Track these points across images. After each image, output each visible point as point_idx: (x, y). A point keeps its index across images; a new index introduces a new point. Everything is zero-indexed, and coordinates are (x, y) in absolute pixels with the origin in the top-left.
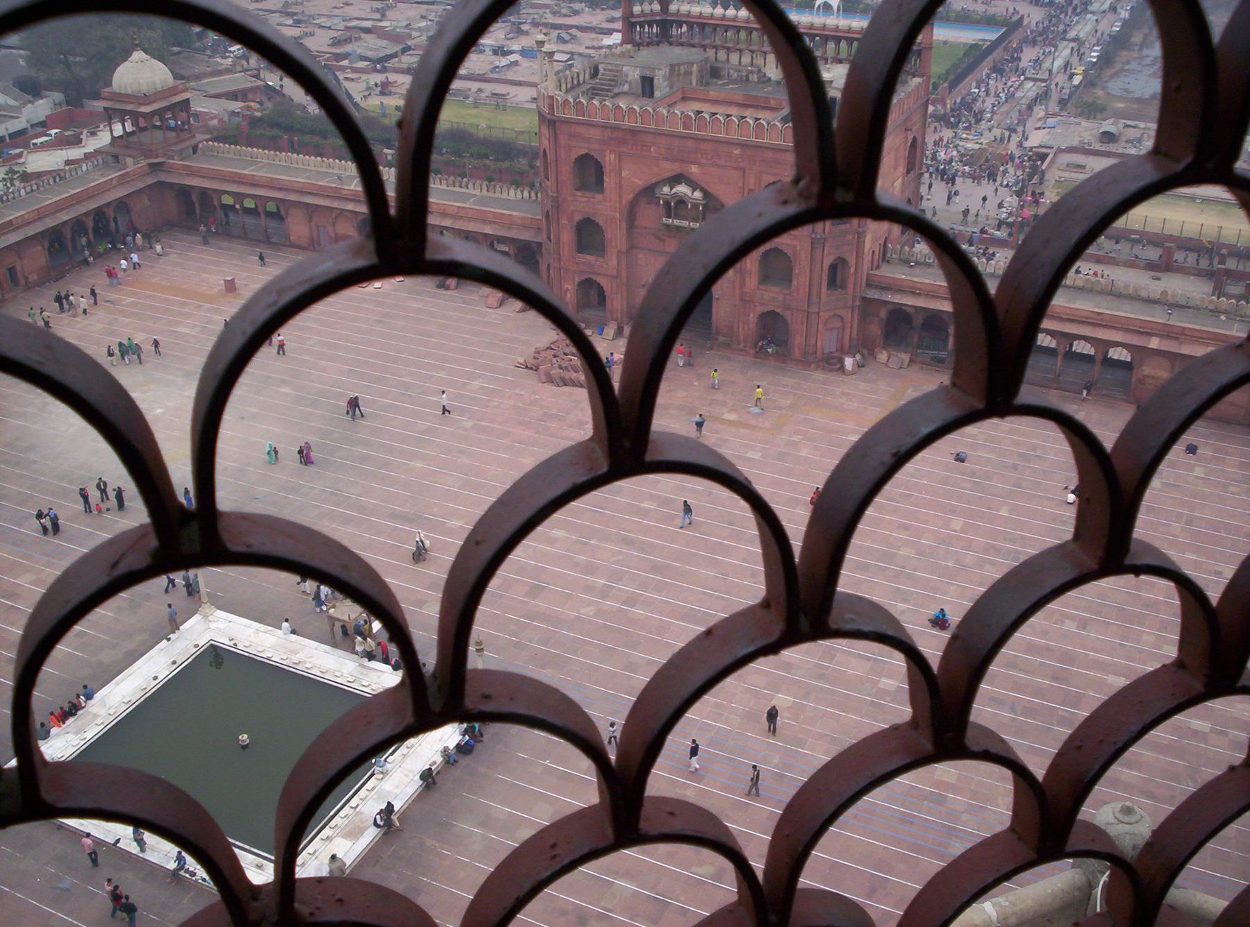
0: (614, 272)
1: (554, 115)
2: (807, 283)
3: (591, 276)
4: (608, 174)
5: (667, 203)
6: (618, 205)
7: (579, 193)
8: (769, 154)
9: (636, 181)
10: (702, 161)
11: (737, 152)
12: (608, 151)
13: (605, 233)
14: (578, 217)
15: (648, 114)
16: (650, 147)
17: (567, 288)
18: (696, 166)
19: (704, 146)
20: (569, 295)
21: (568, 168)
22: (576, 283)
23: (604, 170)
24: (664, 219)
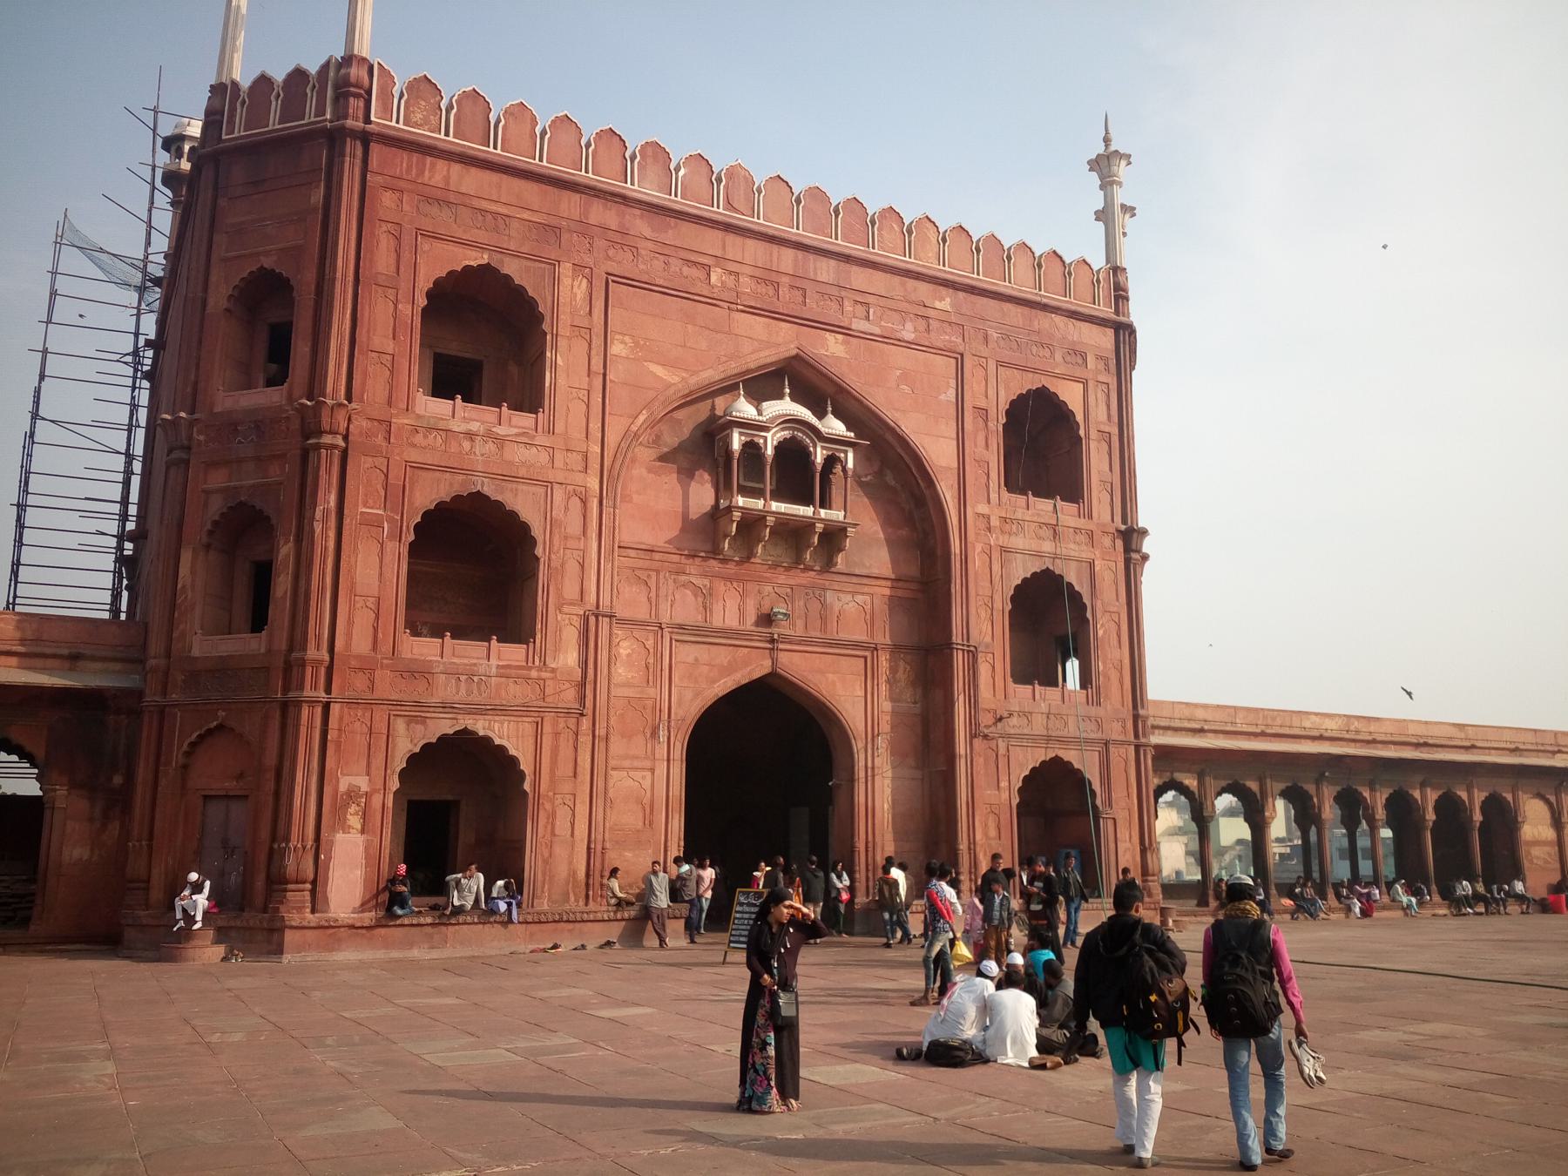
1: (367, 120)
2: (1127, 661)
3: (467, 722)
4: (562, 343)
5: (752, 449)
9: (659, 370)
10: (859, 325)
11: (945, 302)
12: (569, 265)
13: (539, 551)
14: (427, 494)
15: (705, 169)
16: (707, 269)
18: (840, 337)
19: (860, 278)
21: (405, 309)
22: (400, 763)
23: (546, 327)
24: (741, 501)
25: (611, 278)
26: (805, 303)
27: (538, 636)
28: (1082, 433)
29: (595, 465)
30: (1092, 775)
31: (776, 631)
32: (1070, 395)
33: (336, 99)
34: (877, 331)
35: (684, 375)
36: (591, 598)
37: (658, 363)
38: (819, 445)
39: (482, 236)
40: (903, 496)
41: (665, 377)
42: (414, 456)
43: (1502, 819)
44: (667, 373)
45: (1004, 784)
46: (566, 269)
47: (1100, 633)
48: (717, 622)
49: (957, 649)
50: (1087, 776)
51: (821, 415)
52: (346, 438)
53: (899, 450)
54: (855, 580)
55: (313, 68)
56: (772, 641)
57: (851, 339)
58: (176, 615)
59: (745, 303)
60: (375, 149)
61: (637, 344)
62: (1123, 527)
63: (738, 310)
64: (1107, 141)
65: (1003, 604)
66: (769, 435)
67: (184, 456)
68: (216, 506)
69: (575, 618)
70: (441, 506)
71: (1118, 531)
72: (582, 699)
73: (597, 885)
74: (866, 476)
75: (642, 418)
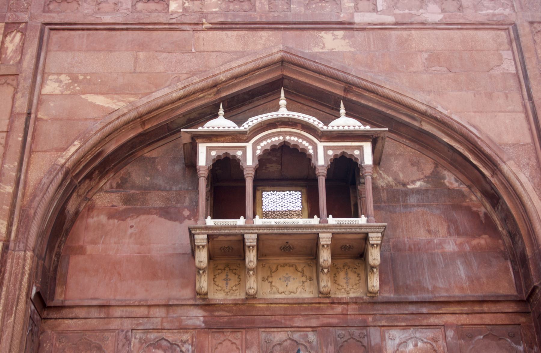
9: (100, 100)
18: (340, 33)
34: (390, 19)
35: (132, 99)
37: (97, 94)
38: (320, 146)
40: (474, 198)
41: (106, 106)
44: (109, 101)
53: (446, 139)
54: (412, 309)
57: (356, 33)
59: (213, 21)
61: (74, 79)
63: (203, 30)
66: (249, 146)
74: (413, 182)
75: (73, 149)
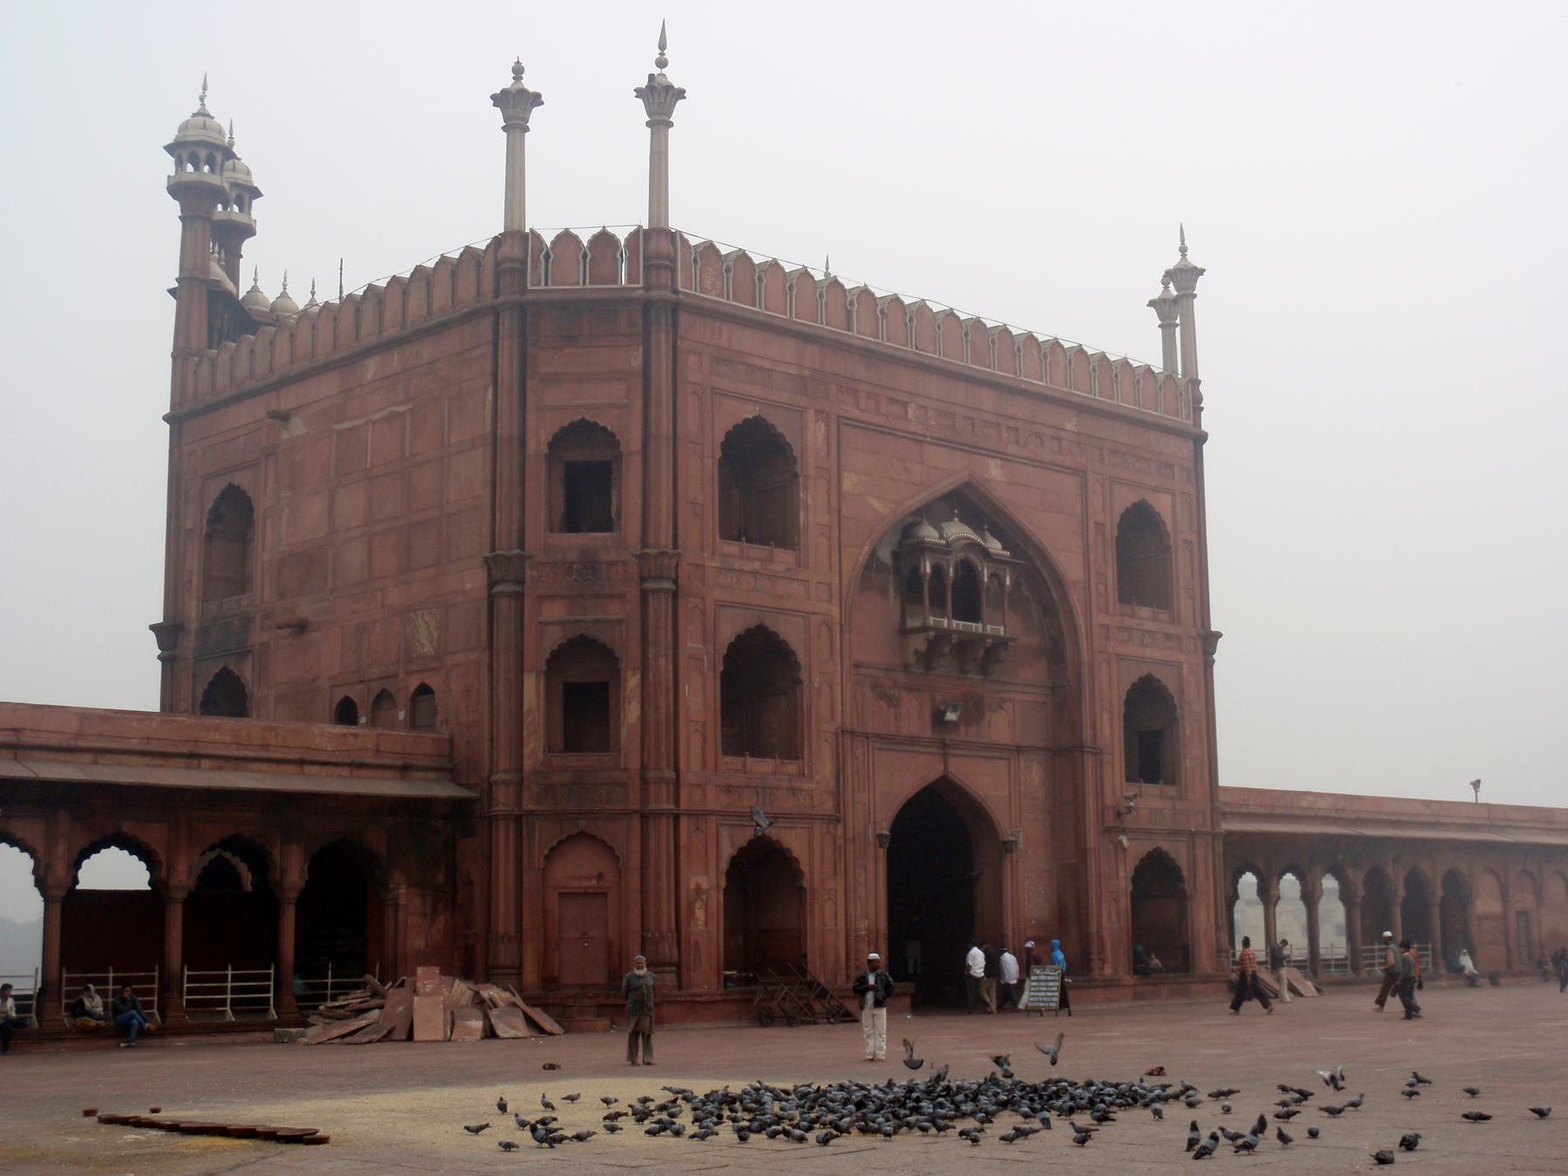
0: (829, 806)
1: (675, 291)
2: (1206, 758)
6: (836, 579)
7: (732, 548)
8: (1122, 434)
10: (1012, 449)
12: (812, 411)
13: (803, 675)
14: (730, 628)
16: (904, 404)
17: (698, 889)
18: (999, 462)
20: (700, 914)
22: (724, 866)
24: (931, 620)
25: (843, 421)
26: (973, 431)
27: (806, 751)
28: (1172, 542)
29: (837, 596)
30: (1183, 863)
31: (948, 738)
32: (1163, 505)
33: (647, 268)
36: (839, 720)
39: (755, 390)
42: (718, 595)
43: (1458, 891)
45: (1122, 874)
46: (810, 415)
47: (1187, 732)
48: (905, 732)
49: (1088, 752)
50: (1179, 863)
51: (981, 534)
52: (675, 581)
55: (622, 235)
56: (945, 746)
58: (525, 734)
60: (684, 318)
62: (1202, 632)
64: (1183, 250)
65: (1119, 709)
67: (517, 588)
68: (554, 638)
69: (828, 734)
70: (739, 638)
71: (1199, 635)
72: (837, 807)
73: (853, 968)
